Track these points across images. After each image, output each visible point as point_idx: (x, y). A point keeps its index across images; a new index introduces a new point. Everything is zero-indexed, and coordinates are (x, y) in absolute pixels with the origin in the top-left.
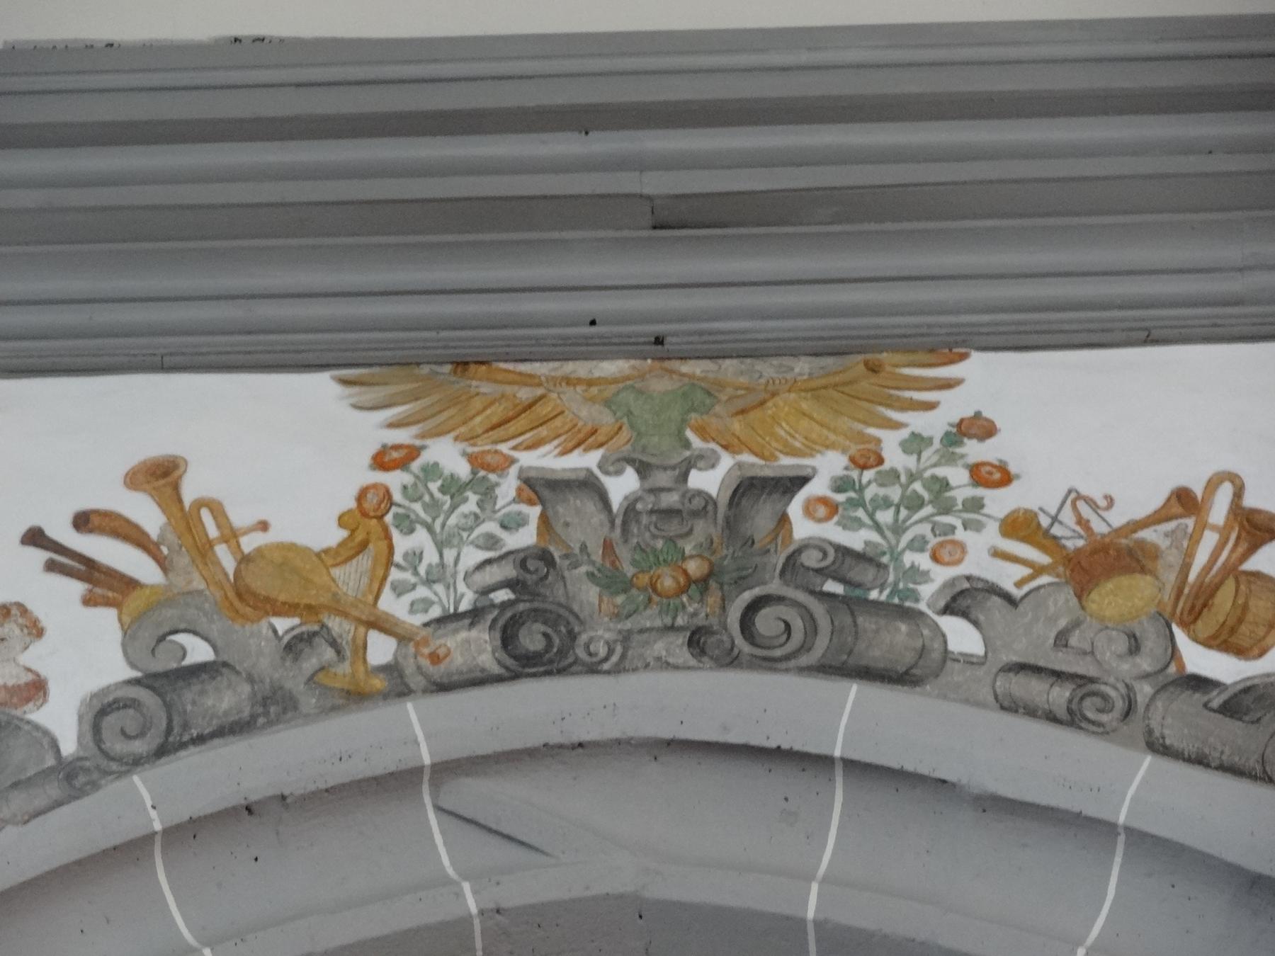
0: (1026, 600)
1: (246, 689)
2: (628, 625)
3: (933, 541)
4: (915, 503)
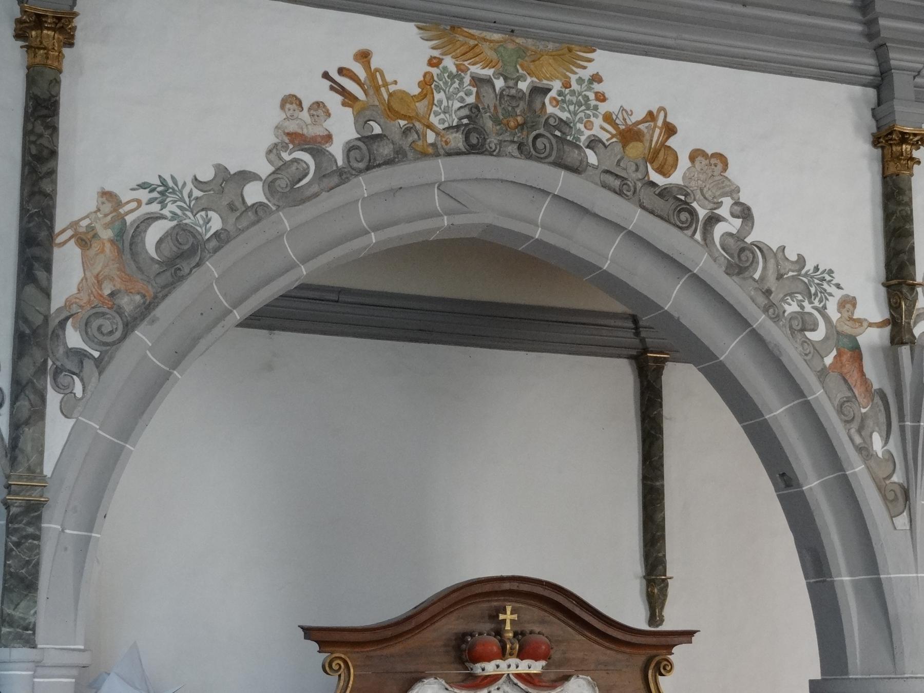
0: (890, 525)
1: (391, 146)
2: (500, 138)
3: (585, 120)
4: (580, 105)
